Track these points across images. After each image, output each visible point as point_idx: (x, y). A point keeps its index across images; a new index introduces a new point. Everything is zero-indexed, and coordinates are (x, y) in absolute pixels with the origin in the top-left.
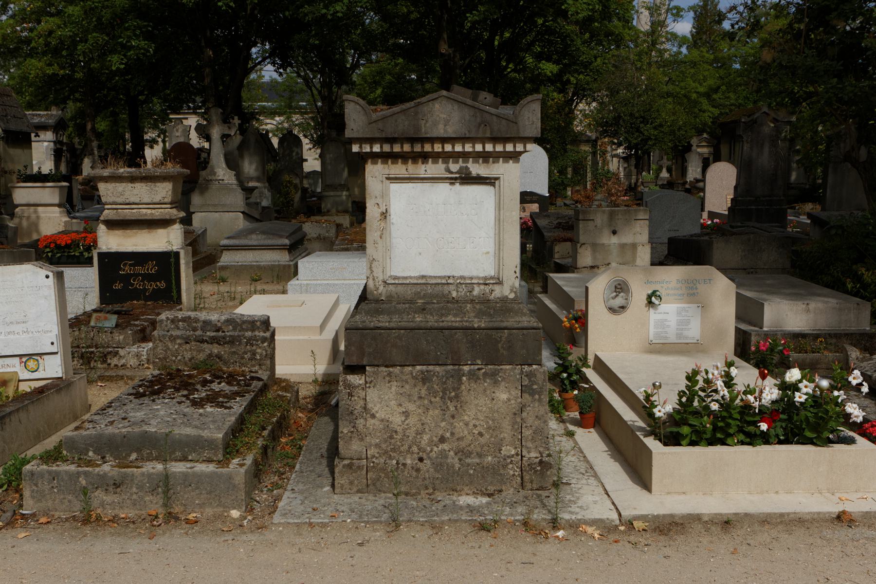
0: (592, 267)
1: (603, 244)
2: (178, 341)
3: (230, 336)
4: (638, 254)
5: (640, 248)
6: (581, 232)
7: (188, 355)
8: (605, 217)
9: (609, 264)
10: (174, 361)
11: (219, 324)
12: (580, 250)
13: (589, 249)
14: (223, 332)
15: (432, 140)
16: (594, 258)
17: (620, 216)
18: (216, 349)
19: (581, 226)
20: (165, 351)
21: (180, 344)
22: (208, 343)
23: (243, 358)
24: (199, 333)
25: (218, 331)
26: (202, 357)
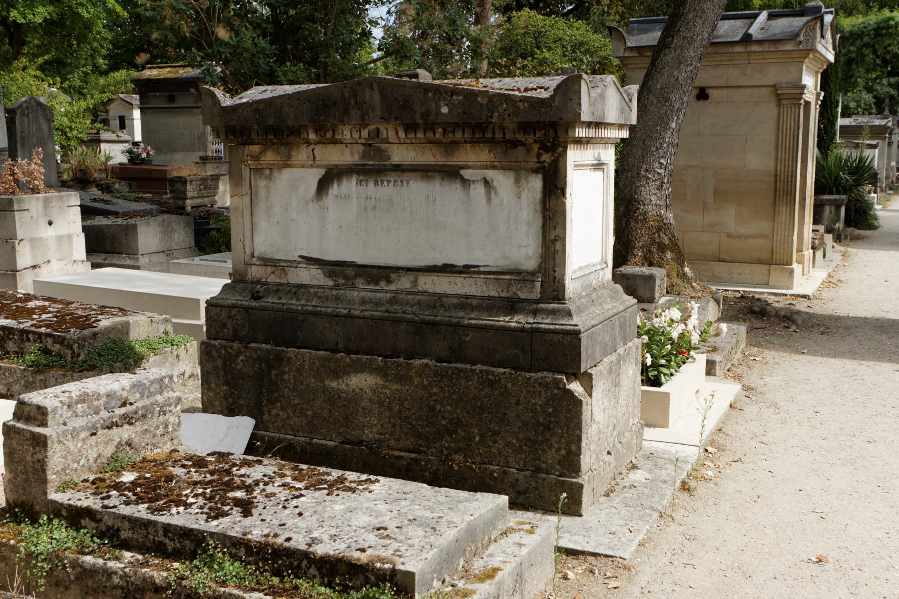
0: (34, 267)
1: (41, 238)
2: (83, 435)
3: (144, 407)
4: (75, 246)
5: (75, 239)
6: (18, 225)
7: (93, 454)
8: (40, 205)
9: (49, 261)
10: (76, 470)
11: (125, 394)
12: (18, 248)
13: (28, 245)
14: (131, 404)
15: (776, 171)
16: (34, 256)
17: (54, 204)
18: (126, 433)
19: (17, 218)
20: (65, 457)
21: (84, 440)
22: (117, 426)
23: (154, 436)
24: (104, 414)
25: (124, 404)
26: (109, 450)
